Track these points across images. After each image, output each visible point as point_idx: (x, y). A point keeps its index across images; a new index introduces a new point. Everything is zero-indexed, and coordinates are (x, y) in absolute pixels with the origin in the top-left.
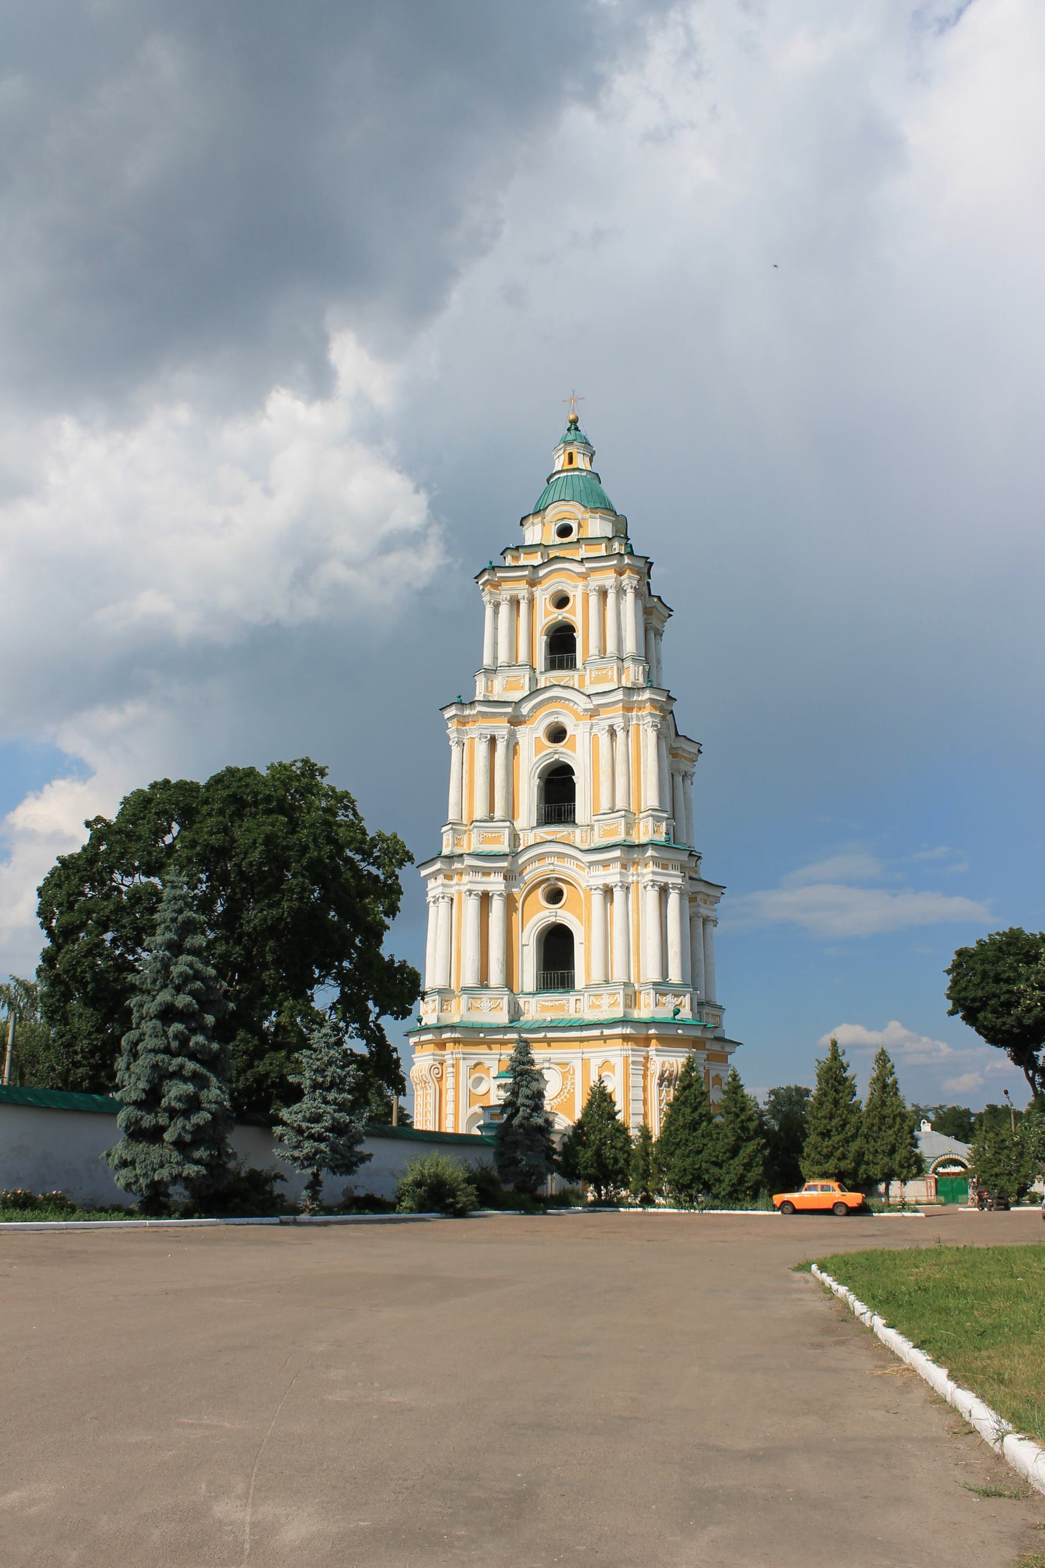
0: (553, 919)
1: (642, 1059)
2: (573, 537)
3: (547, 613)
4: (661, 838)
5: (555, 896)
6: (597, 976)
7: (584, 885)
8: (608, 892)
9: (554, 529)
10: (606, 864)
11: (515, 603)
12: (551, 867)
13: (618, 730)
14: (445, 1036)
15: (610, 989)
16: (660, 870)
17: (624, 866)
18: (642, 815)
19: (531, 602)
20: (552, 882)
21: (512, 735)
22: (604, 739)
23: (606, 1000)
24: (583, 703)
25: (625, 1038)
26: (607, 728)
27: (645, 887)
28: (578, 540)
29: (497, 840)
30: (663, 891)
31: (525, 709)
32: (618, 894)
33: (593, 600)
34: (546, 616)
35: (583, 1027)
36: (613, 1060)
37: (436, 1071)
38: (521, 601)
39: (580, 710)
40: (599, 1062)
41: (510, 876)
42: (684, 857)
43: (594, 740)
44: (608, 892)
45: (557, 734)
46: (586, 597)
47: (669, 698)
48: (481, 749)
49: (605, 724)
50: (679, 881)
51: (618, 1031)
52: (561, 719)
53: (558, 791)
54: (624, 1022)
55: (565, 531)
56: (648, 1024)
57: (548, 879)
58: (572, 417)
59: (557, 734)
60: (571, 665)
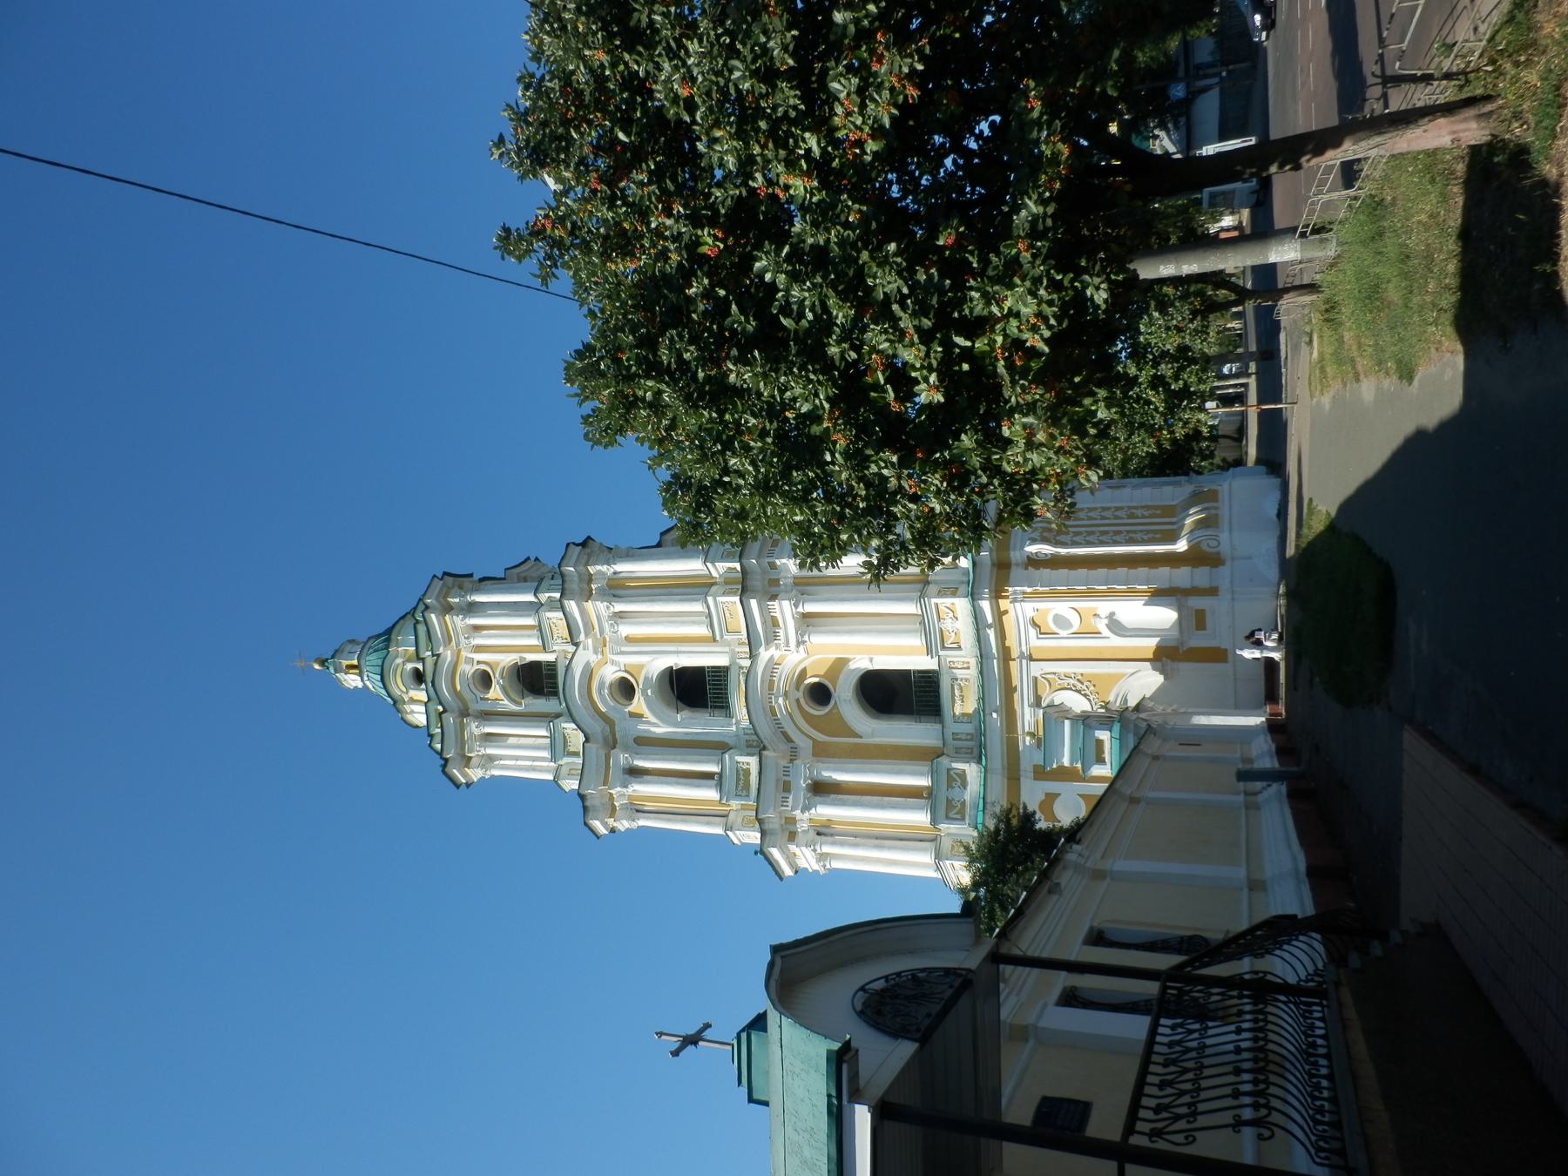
2: (420, 667)
8: (807, 621)
10: (773, 623)
17: (774, 597)
18: (715, 574)
20: (800, 695)
21: (626, 749)
23: (948, 624)
29: (747, 772)
40: (1032, 632)
45: (625, 689)
46: (479, 649)
47: (584, 544)
48: (640, 789)
58: (317, 667)
60: (552, 666)
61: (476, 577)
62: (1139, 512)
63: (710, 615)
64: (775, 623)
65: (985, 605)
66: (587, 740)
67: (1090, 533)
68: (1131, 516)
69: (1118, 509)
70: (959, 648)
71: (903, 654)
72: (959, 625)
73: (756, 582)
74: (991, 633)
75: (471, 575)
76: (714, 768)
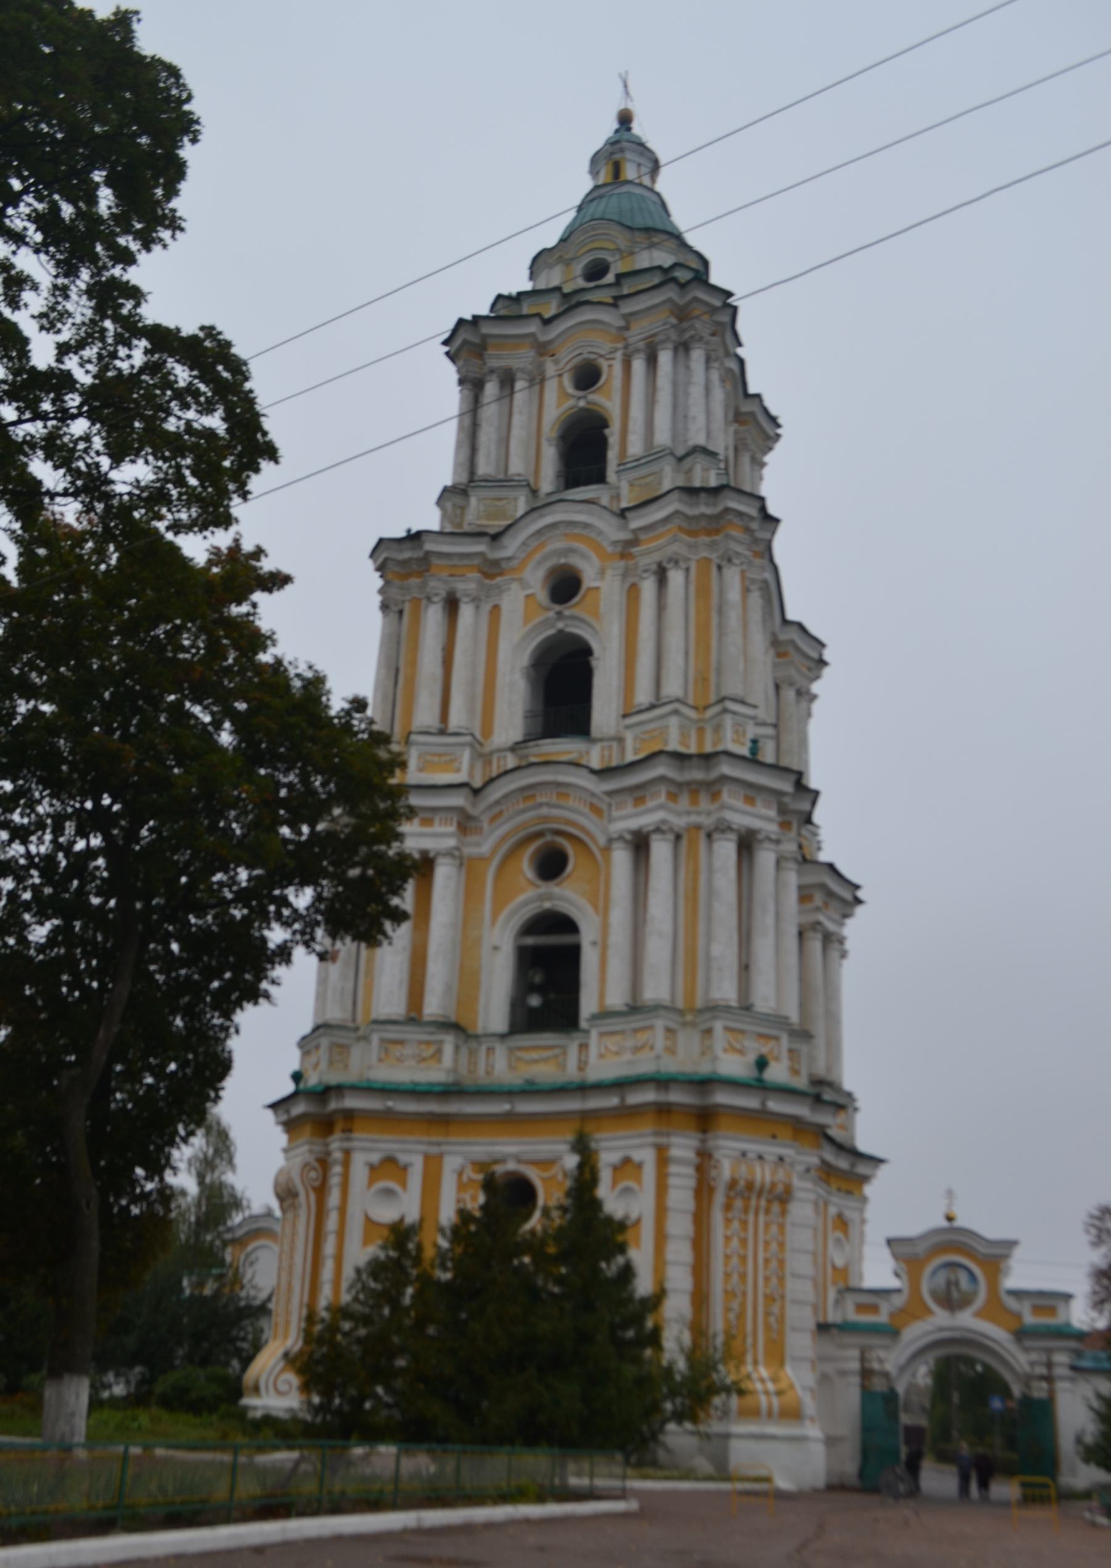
0: (547, 905)
1: (690, 1155)
2: (610, 278)
3: (563, 395)
4: (744, 751)
5: (551, 865)
6: (616, 998)
7: (602, 840)
9: (578, 268)
10: (638, 793)
11: (508, 380)
12: (545, 811)
13: (669, 566)
14: (333, 1105)
15: (636, 1022)
16: (739, 804)
17: (673, 797)
18: (710, 713)
19: (538, 380)
20: (549, 838)
22: (648, 588)
24: (610, 530)
25: (663, 1111)
26: (654, 567)
27: (709, 836)
28: (620, 277)
30: (747, 844)
31: (511, 546)
32: (660, 850)
33: (639, 365)
34: (557, 402)
35: (583, 1089)
36: (637, 1156)
37: (313, 1174)
38: (519, 375)
39: (605, 544)
41: (466, 824)
42: (787, 786)
43: (633, 593)
44: (640, 844)
45: (565, 587)
49: (649, 561)
50: (772, 828)
51: (649, 1096)
52: (576, 561)
53: (563, 686)
54: (662, 1082)
55: (597, 271)
56: (704, 1084)
57: (540, 834)
59: (565, 587)
60: (600, 478)
61: (740, 351)
62: (776, 1309)
63: (652, 707)
64: (639, 801)
65: (649, 1096)
66: (496, 537)
67: (744, 1242)
68: (770, 1299)
69: (781, 1279)
70: (601, 1056)
71: (601, 984)
72: (627, 1056)
73: (697, 774)
74: (613, 1101)
75: (740, 344)
76: (457, 718)
